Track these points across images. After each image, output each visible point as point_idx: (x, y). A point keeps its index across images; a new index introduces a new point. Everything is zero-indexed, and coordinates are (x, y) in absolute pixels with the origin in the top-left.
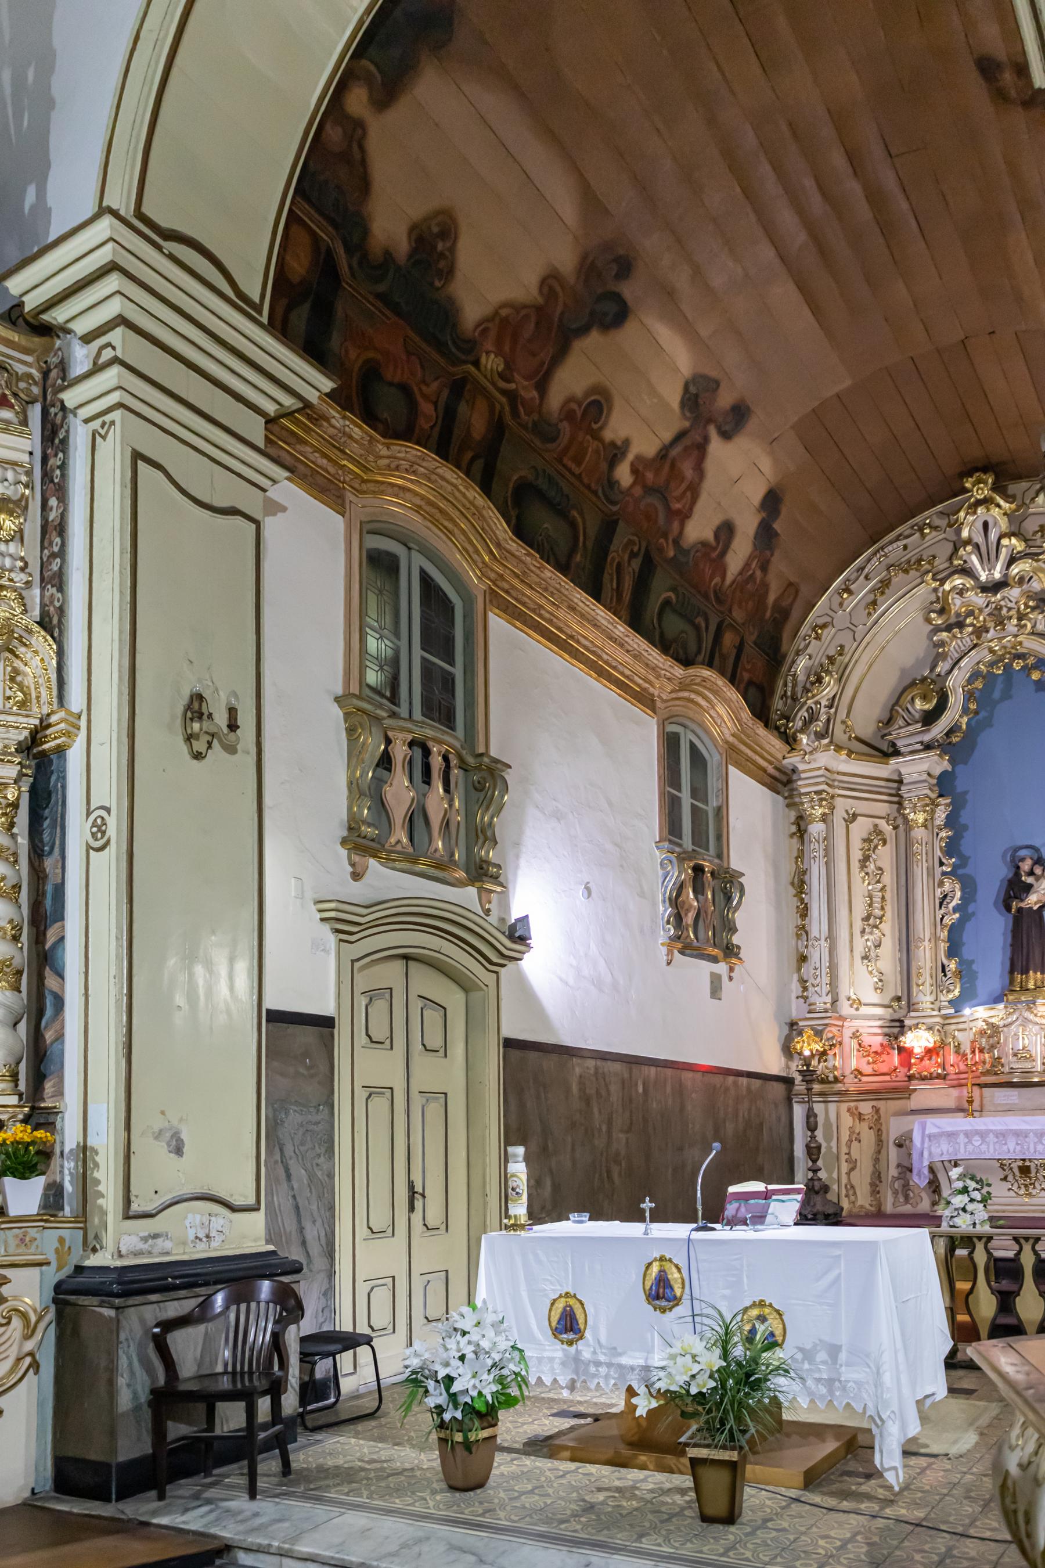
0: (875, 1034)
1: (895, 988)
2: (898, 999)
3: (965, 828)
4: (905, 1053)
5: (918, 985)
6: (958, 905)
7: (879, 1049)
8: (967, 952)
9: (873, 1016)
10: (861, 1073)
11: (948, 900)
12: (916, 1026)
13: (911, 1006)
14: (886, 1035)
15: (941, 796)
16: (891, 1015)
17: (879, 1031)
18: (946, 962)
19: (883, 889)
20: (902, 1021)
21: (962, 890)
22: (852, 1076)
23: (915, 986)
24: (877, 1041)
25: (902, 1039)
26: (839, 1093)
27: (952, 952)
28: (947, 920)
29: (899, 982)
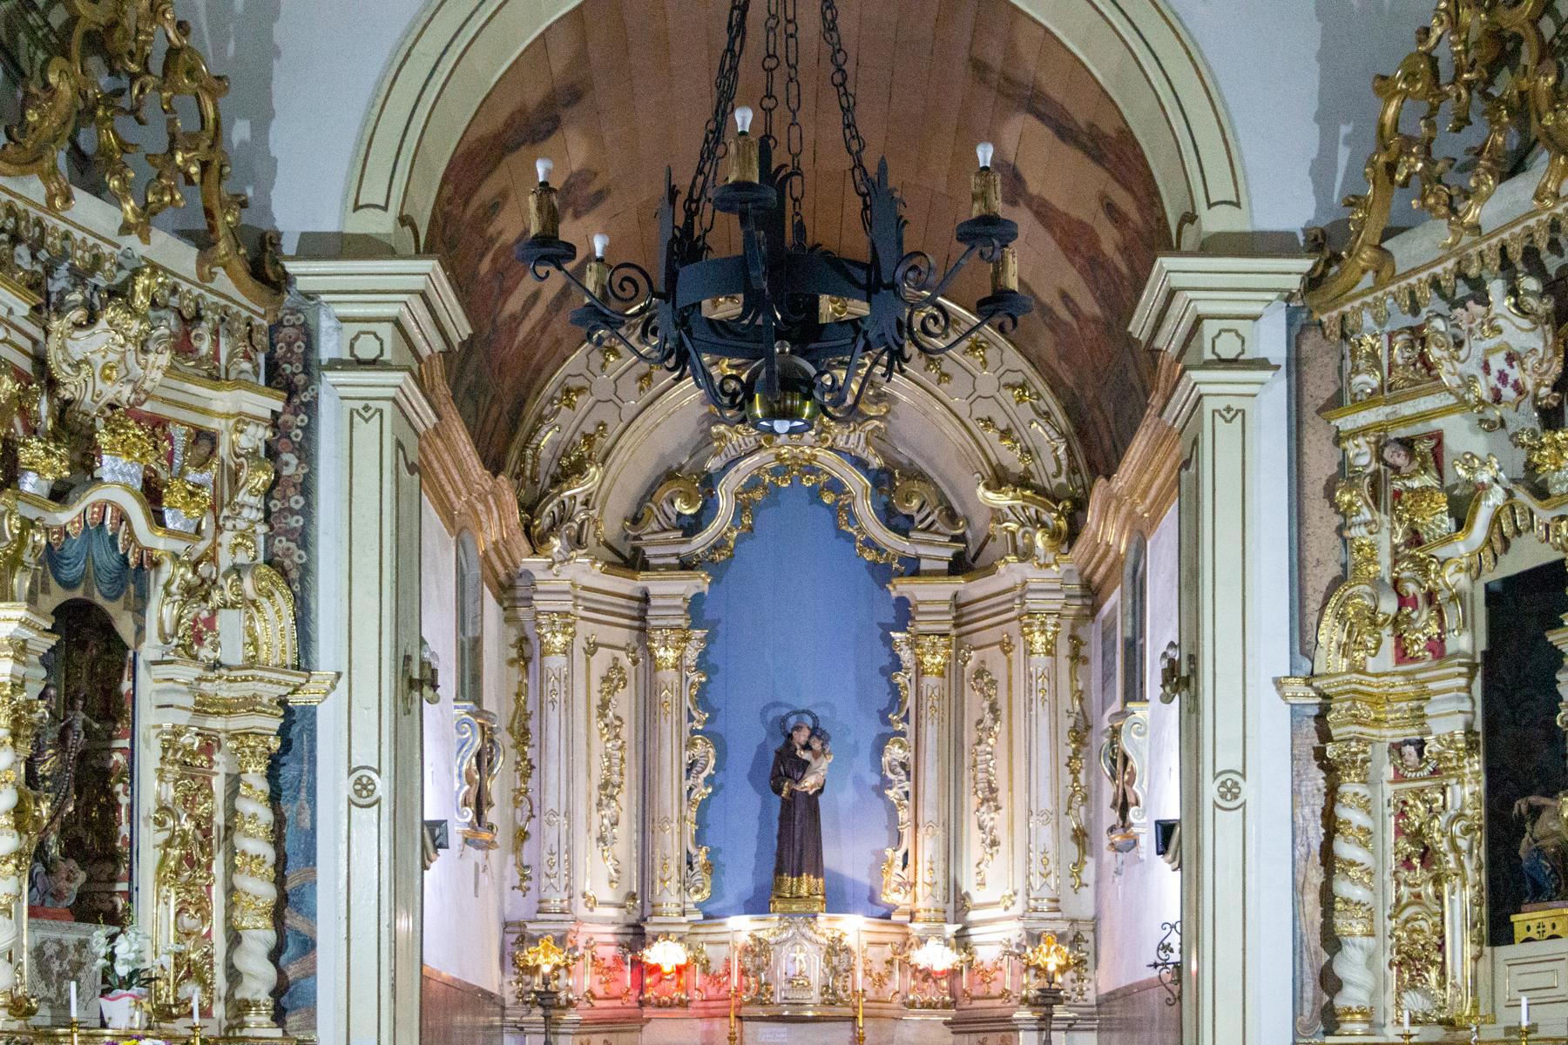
0: (609, 944)
2: (632, 896)
4: (640, 968)
6: (710, 775)
9: (607, 918)
10: (593, 996)
17: (611, 939)
18: (693, 851)
25: (646, 952)
27: (699, 839)
28: (696, 796)
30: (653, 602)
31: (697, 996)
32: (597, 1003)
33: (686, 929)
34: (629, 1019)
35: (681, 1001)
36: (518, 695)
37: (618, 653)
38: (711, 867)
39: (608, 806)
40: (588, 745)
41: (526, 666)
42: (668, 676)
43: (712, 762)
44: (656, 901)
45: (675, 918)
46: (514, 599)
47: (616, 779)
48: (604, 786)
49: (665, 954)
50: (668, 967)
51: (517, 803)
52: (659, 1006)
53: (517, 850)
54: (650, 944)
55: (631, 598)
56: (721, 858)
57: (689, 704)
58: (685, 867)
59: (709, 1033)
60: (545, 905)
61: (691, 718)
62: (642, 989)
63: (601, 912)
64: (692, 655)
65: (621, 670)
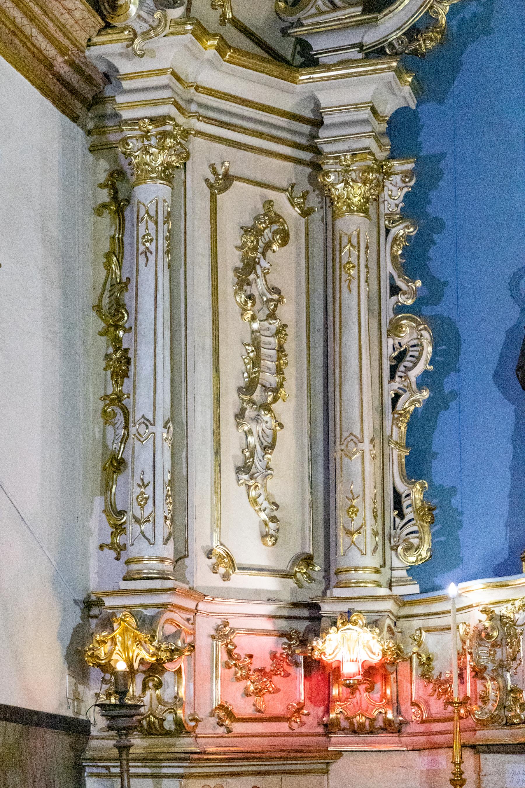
1: (299, 537)
2: (308, 560)
3: (438, 225)
5: (350, 533)
6: (426, 373)
7: (268, 664)
8: (442, 471)
10: (230, 715)
11: (407, 362)
12: (348, 617)
13: (332, 576)
14: (283, 634)
15: (391, 158)
16: (293, 593)
18: (402, 488)
19: (280, 331)
20: (317, 607)
21: (435, 342)
22: (214, 720)
23: (342, 534)
24: (262, 647)
26: (186, 758)
29: (308, 524)
30: (327, 120)
31: (412, 713)
32: (238, 728)
33: (389, 605)
34: (299, 753)
35: (387, 721)
36: (108, 256)
37: (272, 195)
38: (429, 512)
39: (257, 420)
40: (215, 322)
41: (120, 212)
42: (353, 224)
43: (428, 349)
44: (342, 564)
45: (371, 590)
46: (102, 117)
47: (270, 378)
48: (249, 388)
49: (349, 647)
50: (350, 669)
51: (107, 417)
52: (355, 732)
53: (107, 488)
54: (326, 631)
55: (294, 117)
56: (455, 502)
57: (390, 268)
58: (391, 513)
59: (431, 776)
60: (134, 567)
61: (395, 290)
62: (328, 704)
63: (240, 580)
64: (394, 193)
65: (276, 219)
